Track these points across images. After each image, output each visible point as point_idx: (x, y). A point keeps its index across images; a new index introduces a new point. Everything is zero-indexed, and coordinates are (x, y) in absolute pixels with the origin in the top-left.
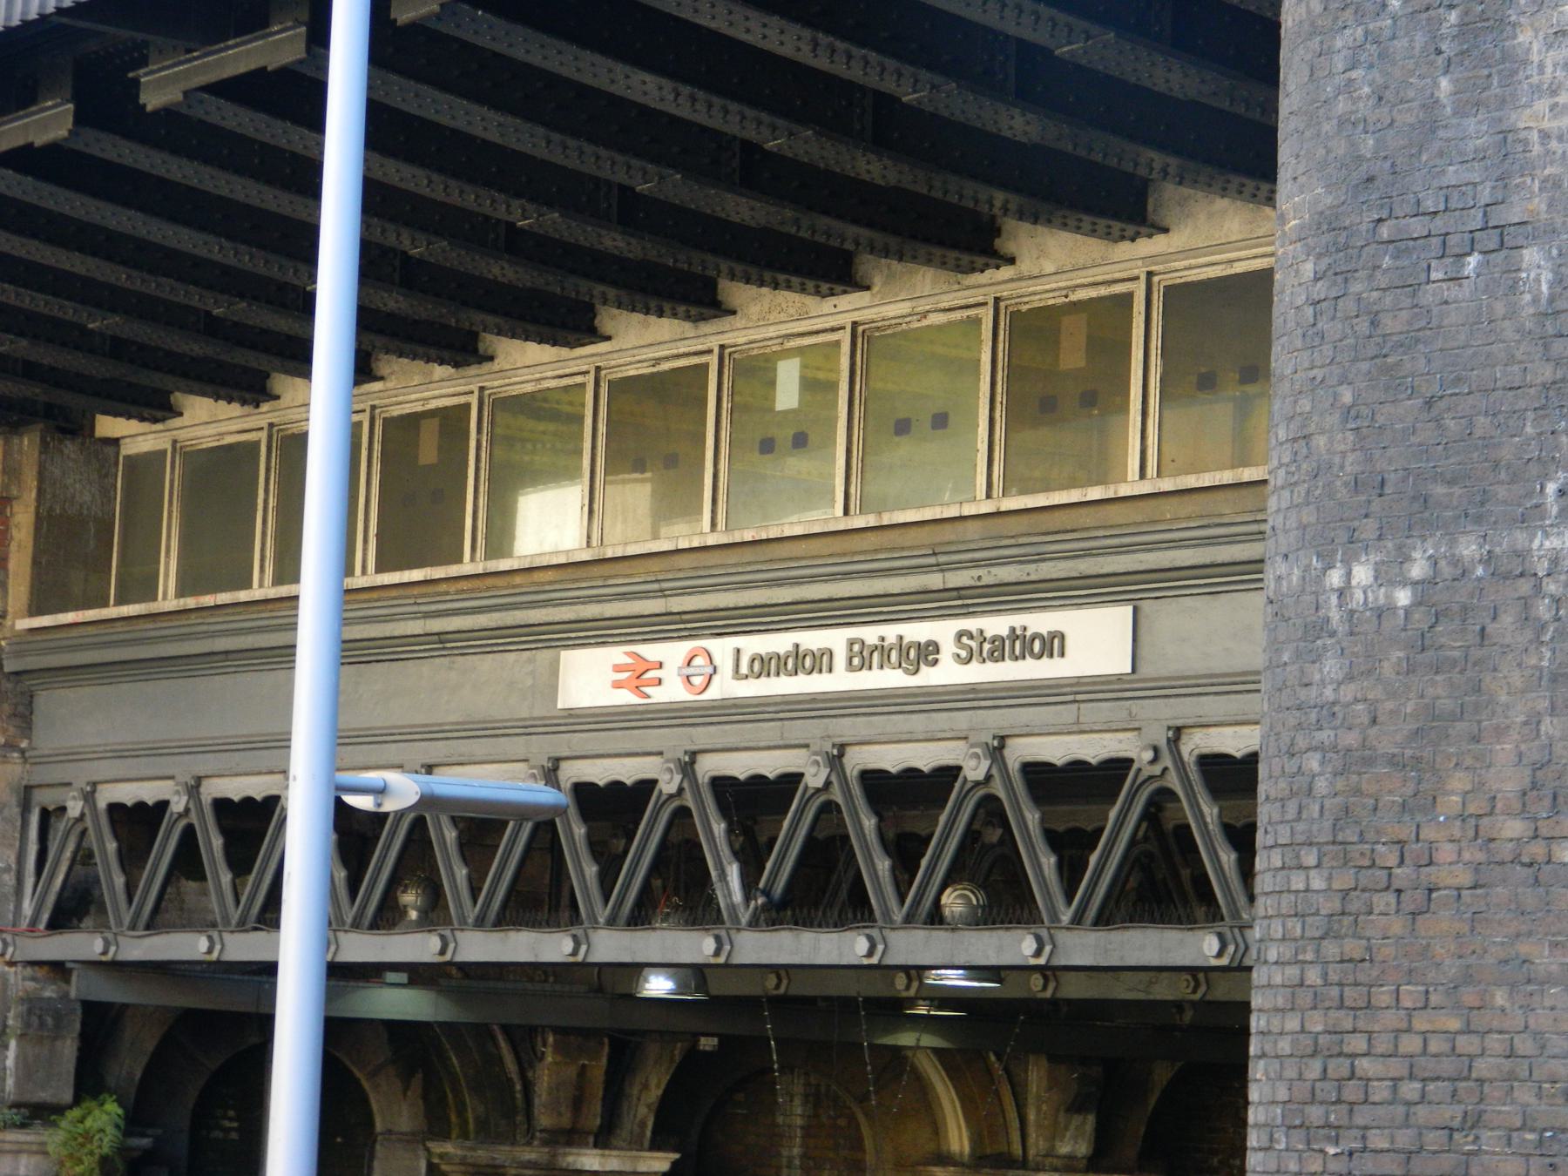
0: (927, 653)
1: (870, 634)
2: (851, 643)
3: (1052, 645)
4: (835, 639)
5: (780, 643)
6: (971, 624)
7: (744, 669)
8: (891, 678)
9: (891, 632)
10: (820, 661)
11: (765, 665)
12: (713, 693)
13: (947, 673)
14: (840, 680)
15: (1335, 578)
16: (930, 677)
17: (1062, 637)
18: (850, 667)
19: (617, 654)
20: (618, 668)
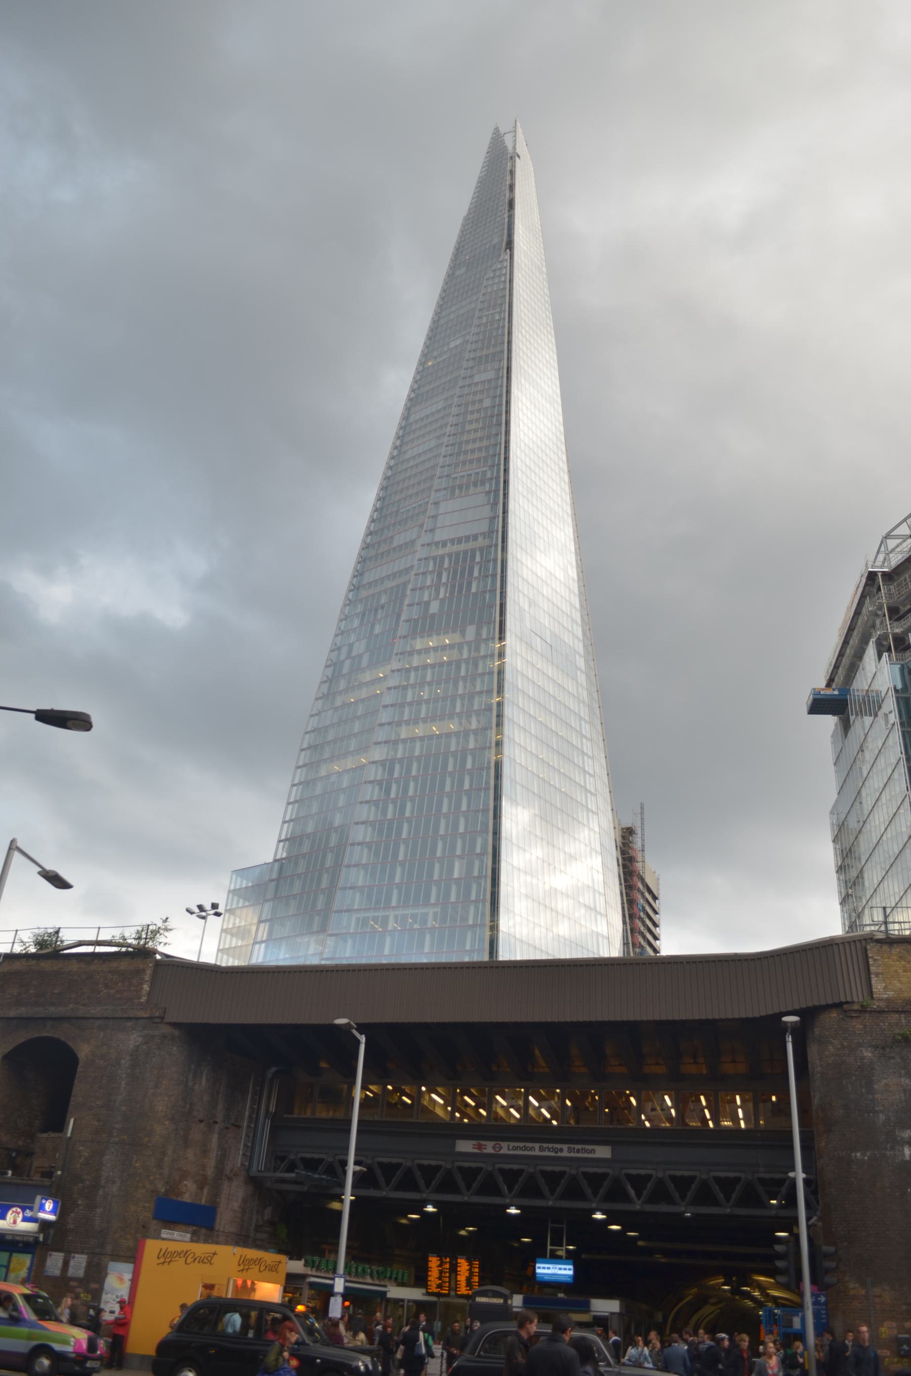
0: (561, 1150)
1: (545, 1145)
2: (540, 1146)
3: (593, 1151)
4: (537, 1146)
5: (521, 1144)
6: (572, 1146)
7: (511, 1148)
8: (553, 1154)
9: (551, 1145)
10: (532, 1149)
11: (516, 1148)
12: (502, 1152)
13: (565, 1154)
14: (537, 1153)
15: (853, 1154)
16: (559, 1154)
17: (594, 1150)
18: (540, 1151)
19: (474, 1142)
20: (474, 1145)
